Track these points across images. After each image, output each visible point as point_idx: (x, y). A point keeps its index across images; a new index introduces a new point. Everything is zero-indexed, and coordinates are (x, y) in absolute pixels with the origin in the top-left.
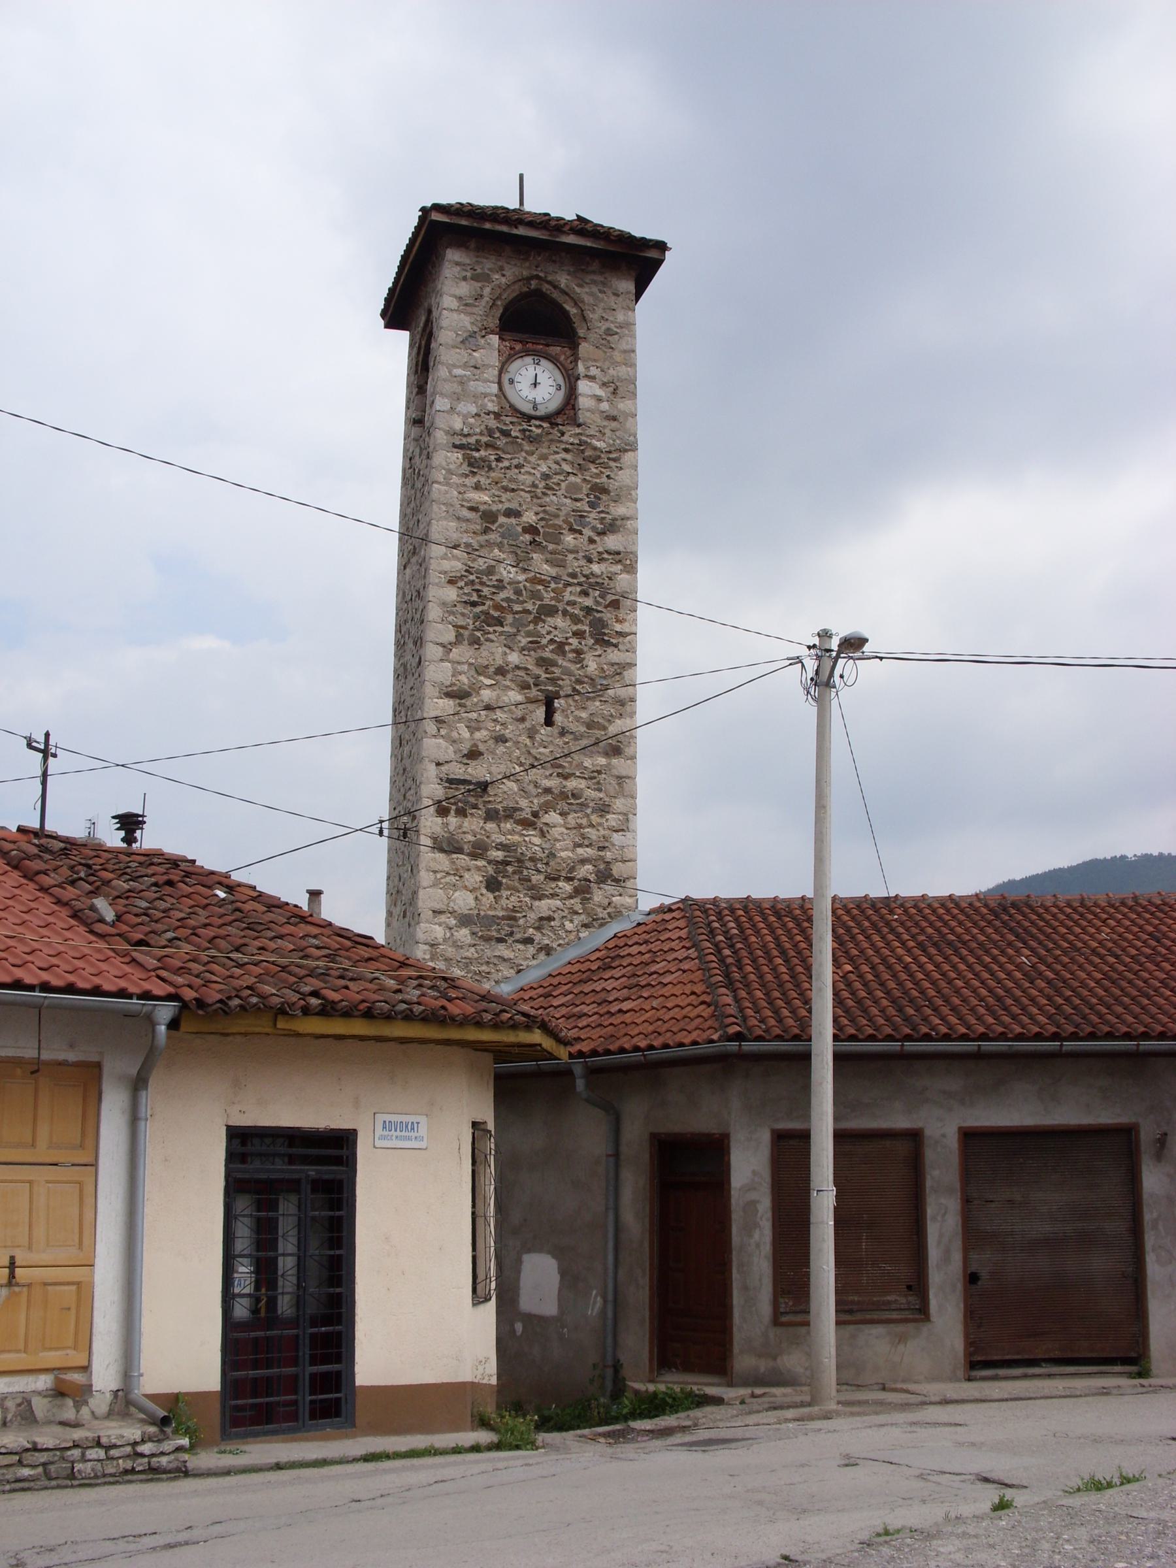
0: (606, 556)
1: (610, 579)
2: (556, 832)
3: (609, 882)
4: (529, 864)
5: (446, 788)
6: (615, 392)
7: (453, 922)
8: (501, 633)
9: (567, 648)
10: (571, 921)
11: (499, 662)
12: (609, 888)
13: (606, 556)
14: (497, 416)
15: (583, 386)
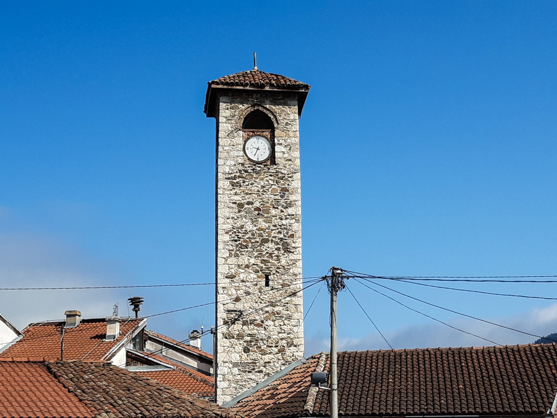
0: (288, 217)
1: (290, 226)
4: (260, 341)
7: (231, 366)
8: (247, 251)
9: (273, 255)
11: (247, 263)
12: (292, 348)
13: (288, 217)
14: (243, 164)
15: (277, 148)
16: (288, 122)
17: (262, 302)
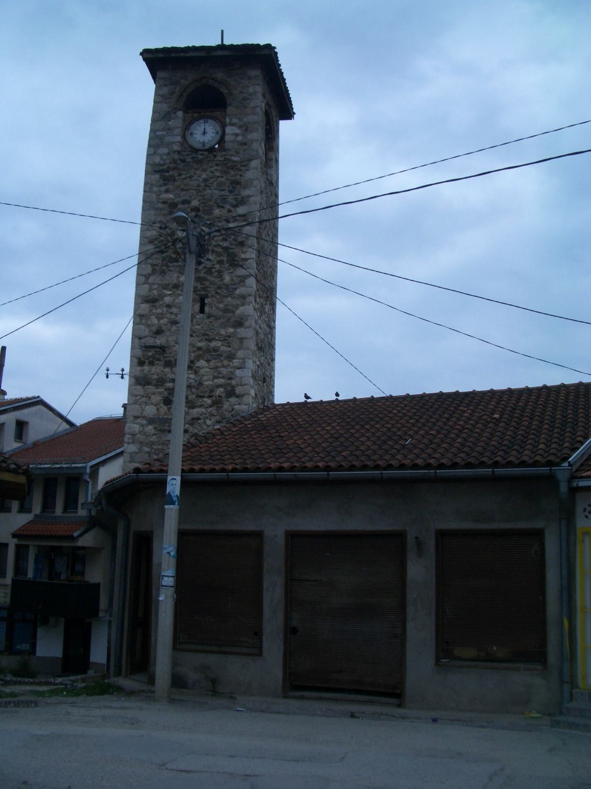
2: (202, 371)
3: (233, 396)
5: (143, 351)
6: (246, 130)
7: (145, 422)
8: (177, 266)
9: (213, 270)
10: (210, 420)
11: (175, 281)
12: (233, 400)
13: (238, 218)
15: (228, 130)
16: (246, 95)
17: (194, 335)
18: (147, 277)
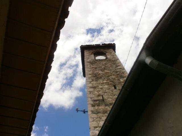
18: (90, 82)
